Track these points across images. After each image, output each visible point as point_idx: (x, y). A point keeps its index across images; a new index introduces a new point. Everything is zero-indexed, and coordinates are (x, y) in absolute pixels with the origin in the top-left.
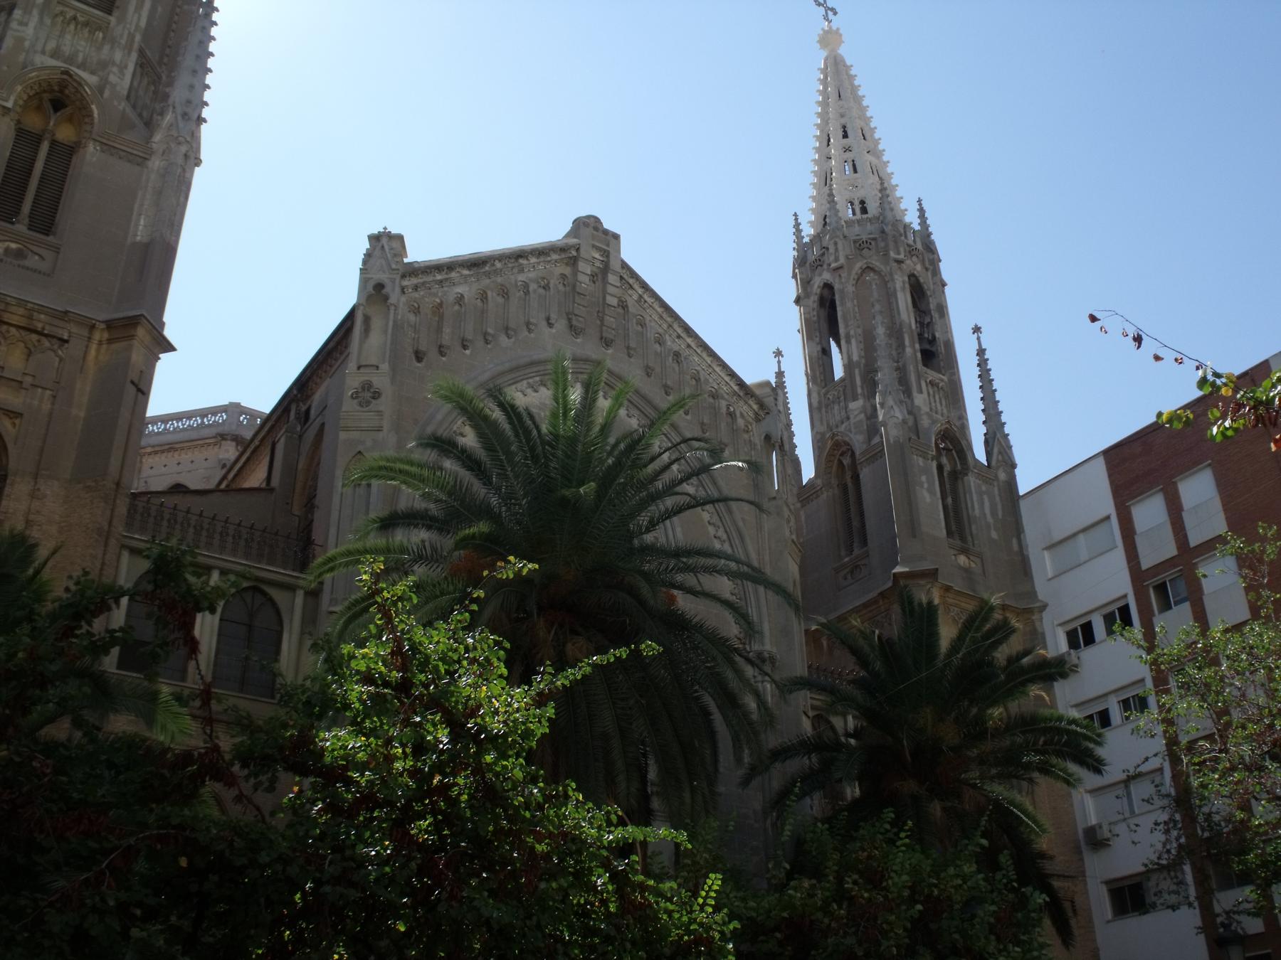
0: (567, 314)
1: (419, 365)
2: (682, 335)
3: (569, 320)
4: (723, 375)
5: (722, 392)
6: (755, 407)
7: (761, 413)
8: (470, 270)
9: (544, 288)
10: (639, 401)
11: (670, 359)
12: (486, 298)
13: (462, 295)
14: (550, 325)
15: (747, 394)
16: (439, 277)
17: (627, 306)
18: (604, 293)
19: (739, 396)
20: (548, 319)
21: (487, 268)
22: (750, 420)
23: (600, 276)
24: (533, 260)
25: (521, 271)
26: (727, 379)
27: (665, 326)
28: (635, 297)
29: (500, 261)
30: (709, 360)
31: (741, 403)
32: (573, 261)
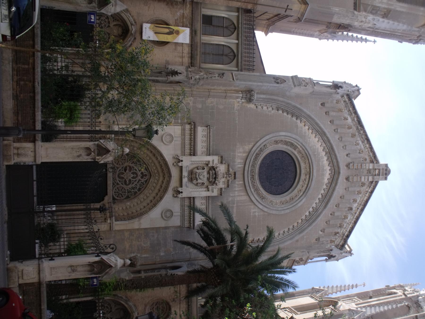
0: (353, 162)
1: (320, 104)
2: (359, 210)
3: (351, 163)
4: (349, 228)
5: (343, 229)
6: (341, 244)
7: (339, 247)
8: (357, 121)
9: (359, 152)
10: (330, 193)
11: (349, 206)
12: (349, 129)
13: (347, 120)
14: (347, 155)
15: (345, 239)
16: (351, 109)
17: (363, 187)
18: (365, 176)
19: (343, 236)
20: (349, 154)
21: (359, 127)
22: (336, 243)
23: (370, 174)
24: (367, 146)
25: (363, 142)
26: (348, 230)
27: (360, 203)
28: (367, 190)
29: (363, 132)
30: (353, 222)
31: (341, 239)
32: (372, 162)
